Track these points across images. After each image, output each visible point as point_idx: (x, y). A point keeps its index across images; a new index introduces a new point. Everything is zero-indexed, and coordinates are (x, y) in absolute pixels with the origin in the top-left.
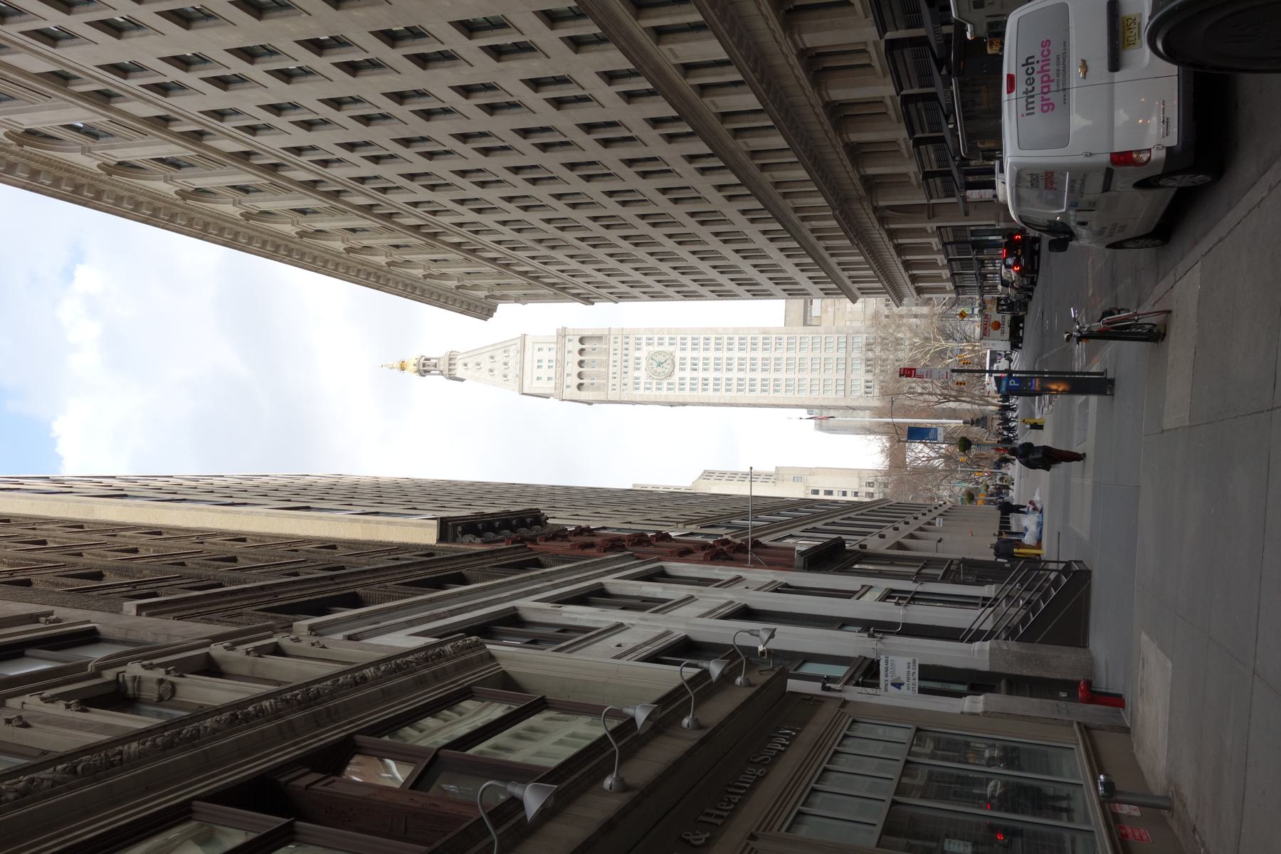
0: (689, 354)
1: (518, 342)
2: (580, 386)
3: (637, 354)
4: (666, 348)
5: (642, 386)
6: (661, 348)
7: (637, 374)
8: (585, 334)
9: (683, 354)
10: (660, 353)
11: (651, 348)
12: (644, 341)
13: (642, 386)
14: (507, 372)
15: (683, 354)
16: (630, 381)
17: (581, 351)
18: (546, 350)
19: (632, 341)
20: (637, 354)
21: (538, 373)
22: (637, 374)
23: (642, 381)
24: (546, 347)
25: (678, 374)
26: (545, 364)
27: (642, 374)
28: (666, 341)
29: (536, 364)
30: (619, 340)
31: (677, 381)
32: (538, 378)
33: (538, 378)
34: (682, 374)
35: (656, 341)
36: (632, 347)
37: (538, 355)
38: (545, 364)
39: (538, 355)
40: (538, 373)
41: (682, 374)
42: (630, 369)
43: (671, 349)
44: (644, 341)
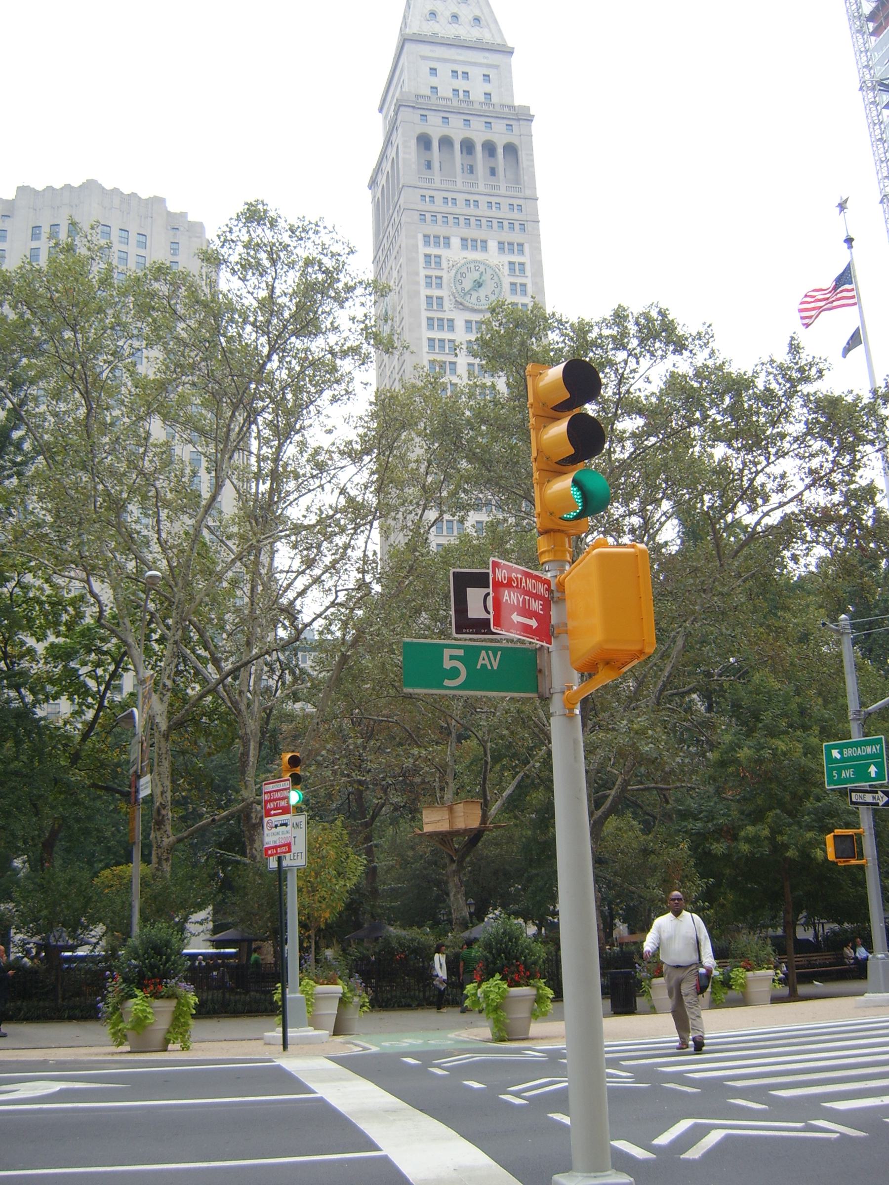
1: (499, 41)
3: (493, 245)
7: (455, 242)
8: (522, 155)
10: (499, 284)
11: (506, 270)
16: (439, 229)
18: (488, 88)
19: (516, 237)
20: (493, 245)
21: (444, 70)
22: (455, 242)
26: (461, 84)
29: (460, 69)
30: (516, 215)
31: (446, 315)
32: (433, 71)
33: (433, 71)
35: (519, 280)
37: (476, 73)
38: (461, 84)
39: (476, 73)
40: (444, 70)
41: (460, 324)
44: (516, 259)
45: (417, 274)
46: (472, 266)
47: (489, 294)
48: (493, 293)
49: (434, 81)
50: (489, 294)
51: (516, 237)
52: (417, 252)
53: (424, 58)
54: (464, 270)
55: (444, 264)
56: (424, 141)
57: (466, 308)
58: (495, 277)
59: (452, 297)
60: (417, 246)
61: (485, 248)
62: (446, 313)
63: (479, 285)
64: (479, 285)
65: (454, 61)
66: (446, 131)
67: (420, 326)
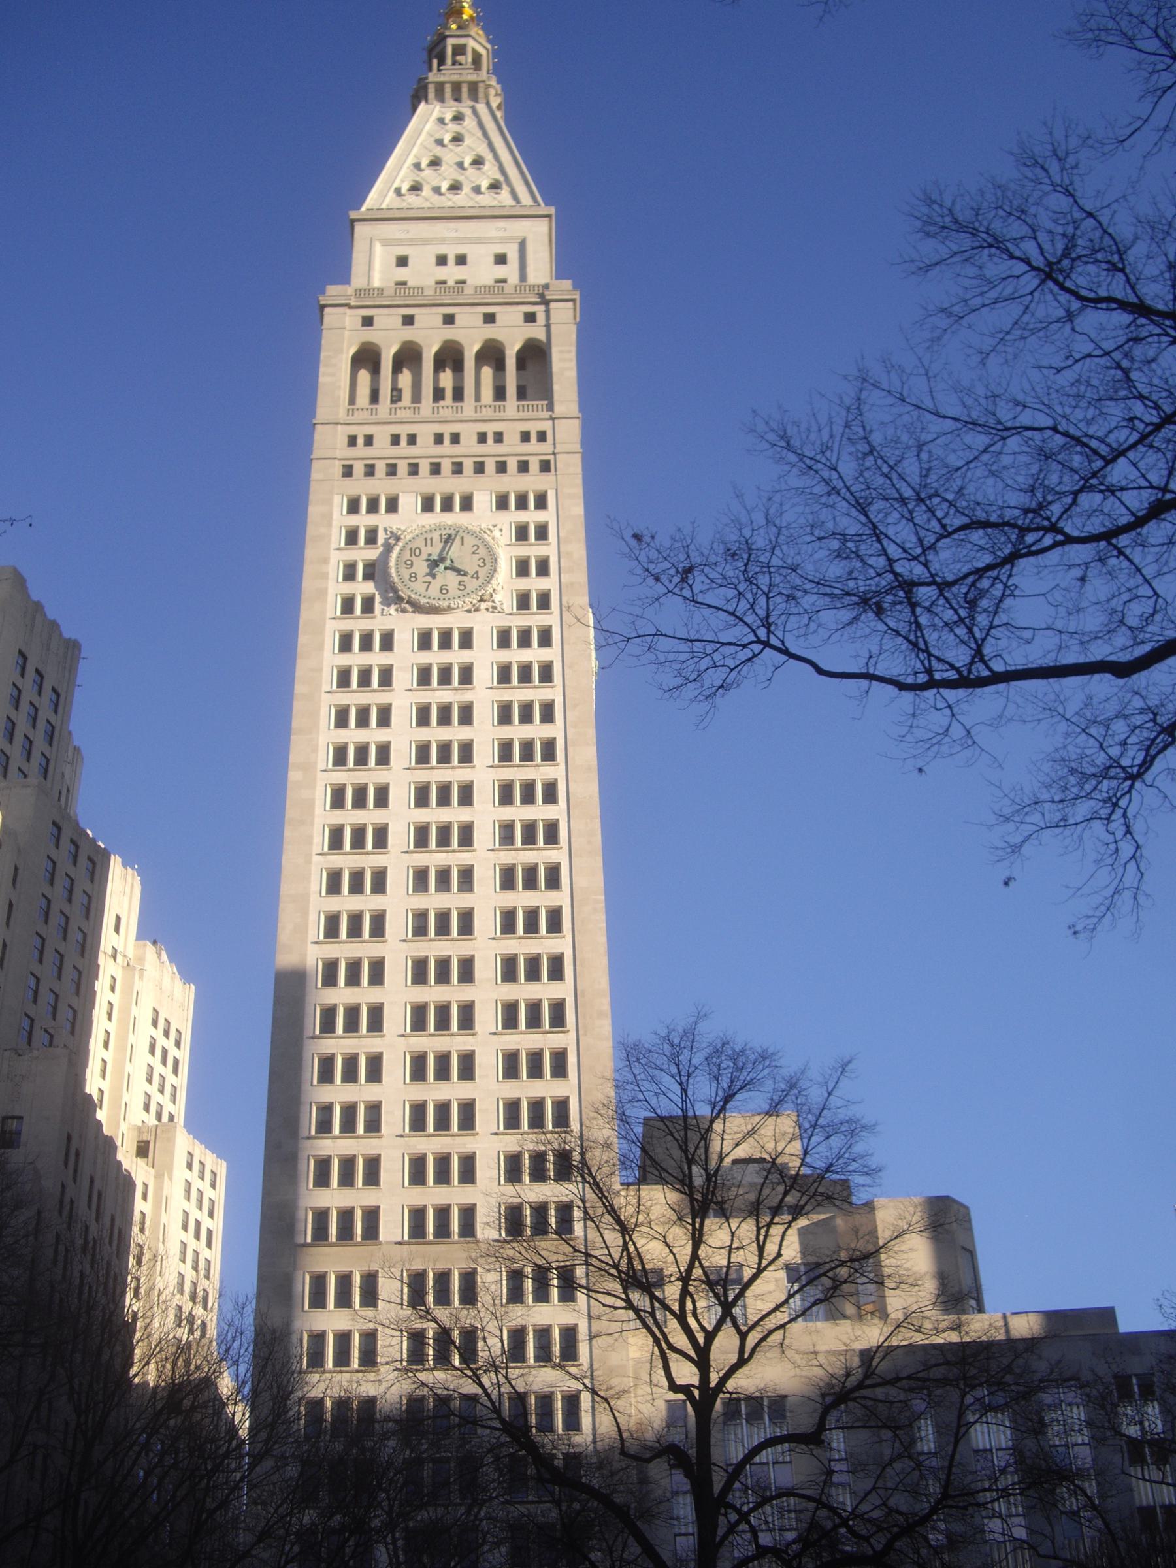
3: (483, 501)
7: (409, 503)
9: (484, 639)
11: (509, 535)
12: (532, 516)
13: (363, 520)
14: (426, 191)
15: (484, 639)
17: (492, 354)
20: (483, 501)
22: (409, 503)
23: (383, 520)
24: (510, 271)
25: (406, 626)
26: (451, 273)
28: (534, 584)
29: (451, 253)
36: (513, 483)
38: (451, 273)
42: (427, 483)
43: (505, 598)
44: (532, 516)
45: (326, 561)
51: (533, 482)
52: (330, 525)
53: (386, 243)
54: (420, 543)
55: (381, 539)
57: (418, 608)
58: (482, 552)
60: (331, 515)
61: (467, 504)
62: (375, 621)
65: (443, 241)
67: (321, 647)
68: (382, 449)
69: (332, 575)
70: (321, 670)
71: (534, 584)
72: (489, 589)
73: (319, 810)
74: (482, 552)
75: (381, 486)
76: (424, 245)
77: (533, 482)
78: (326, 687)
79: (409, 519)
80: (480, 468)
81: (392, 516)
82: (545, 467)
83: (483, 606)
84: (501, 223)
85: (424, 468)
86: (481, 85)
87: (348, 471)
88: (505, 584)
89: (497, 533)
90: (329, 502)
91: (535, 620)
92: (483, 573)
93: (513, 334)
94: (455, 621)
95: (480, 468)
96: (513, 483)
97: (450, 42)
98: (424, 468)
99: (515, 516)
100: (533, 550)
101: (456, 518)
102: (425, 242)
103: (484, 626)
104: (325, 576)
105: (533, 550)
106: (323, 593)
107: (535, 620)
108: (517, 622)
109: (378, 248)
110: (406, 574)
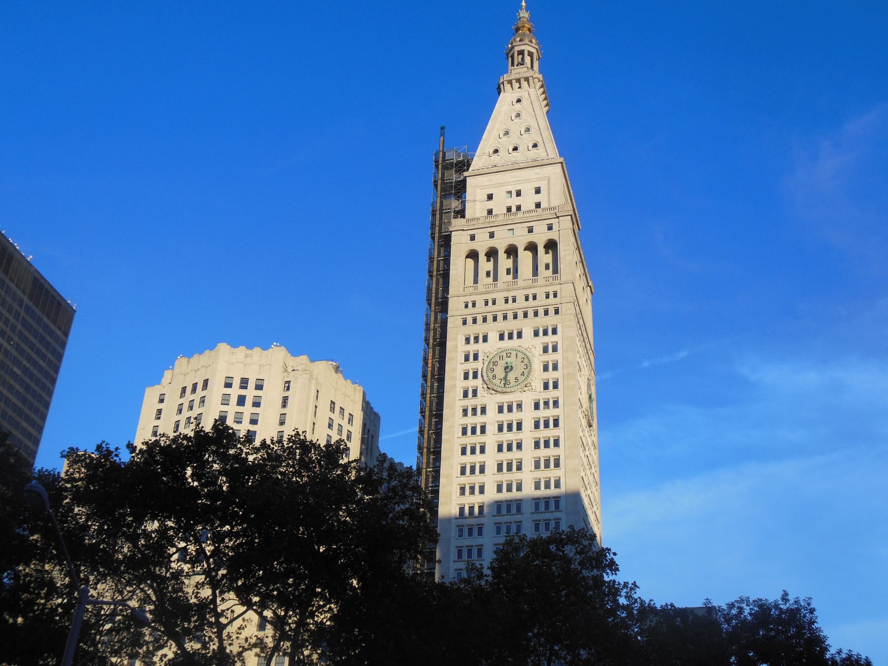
0: (528, 416)
2: (473, 255)
3: (528, 332)
4: (538, 377)
5: (472, 348)
6: (537, 366)
7: (493, 336)
9: (528, 406)
10: (528, 366)
12: (550, 339)
16: (480, 329)
17: (532, 247)
20: (528, 332)
22: (493, 336)
23: (481, 347)
25: (491, 401)
26: (514, 201)
27: (494, 345)
28: (551, 375)
31: (478, 402)
34: (492, 410)
36: (542, 322)
37: (528, 191)
42: (501, 325)
45: (455, 370)
46: (504, 354)
47: (519, 376)
48: (523, 374)
49: (490, 205)
50: (519, 376)
51: (551, 320)
52: (456, 351)
53: (483, 187)
55: (480, 357)
56: (473, 255)
58: (526, 361)
59: (485, 386)
63: (508, 369)
64: (508, 369)
66: (492, 243)
67: (454, 415)
68: (480, 308)
69: (458, 377)
70: (453, 427)
71: (551, 375)
72: (529, 380)
73: (454, 497)
74: (526, 361)
75: (480, 329)
76: (501, 185)
77: (551, 320)
78: (456, 436)
79: (494, 345)
80: (526, 315)
81: (485, 344)
82: (557, 312)
83: (526, 389)
84: (537, 170)
85: (500, 317)
86: (531, 79)
87: (465, 323)
88: (538, 377)
89: (533, 350)
90: (456, 339)
91: (551, 394)
92: (526, 372)
93: (541, 237)
94: (512, 398)
95: (526, 315)
96: (542, 322)
97: (517, 49)
98: (500, 317)
99: (542, 339)
100: (551, 357)
101: (515, 343)
102: (500, 185)
103: (528, 400)
104: (454, 378)
105: (551, 357)
106: (454, 386)
107: (551, 394)
108: (543, 396)
109: (478, 190)
110: (491, 375)
